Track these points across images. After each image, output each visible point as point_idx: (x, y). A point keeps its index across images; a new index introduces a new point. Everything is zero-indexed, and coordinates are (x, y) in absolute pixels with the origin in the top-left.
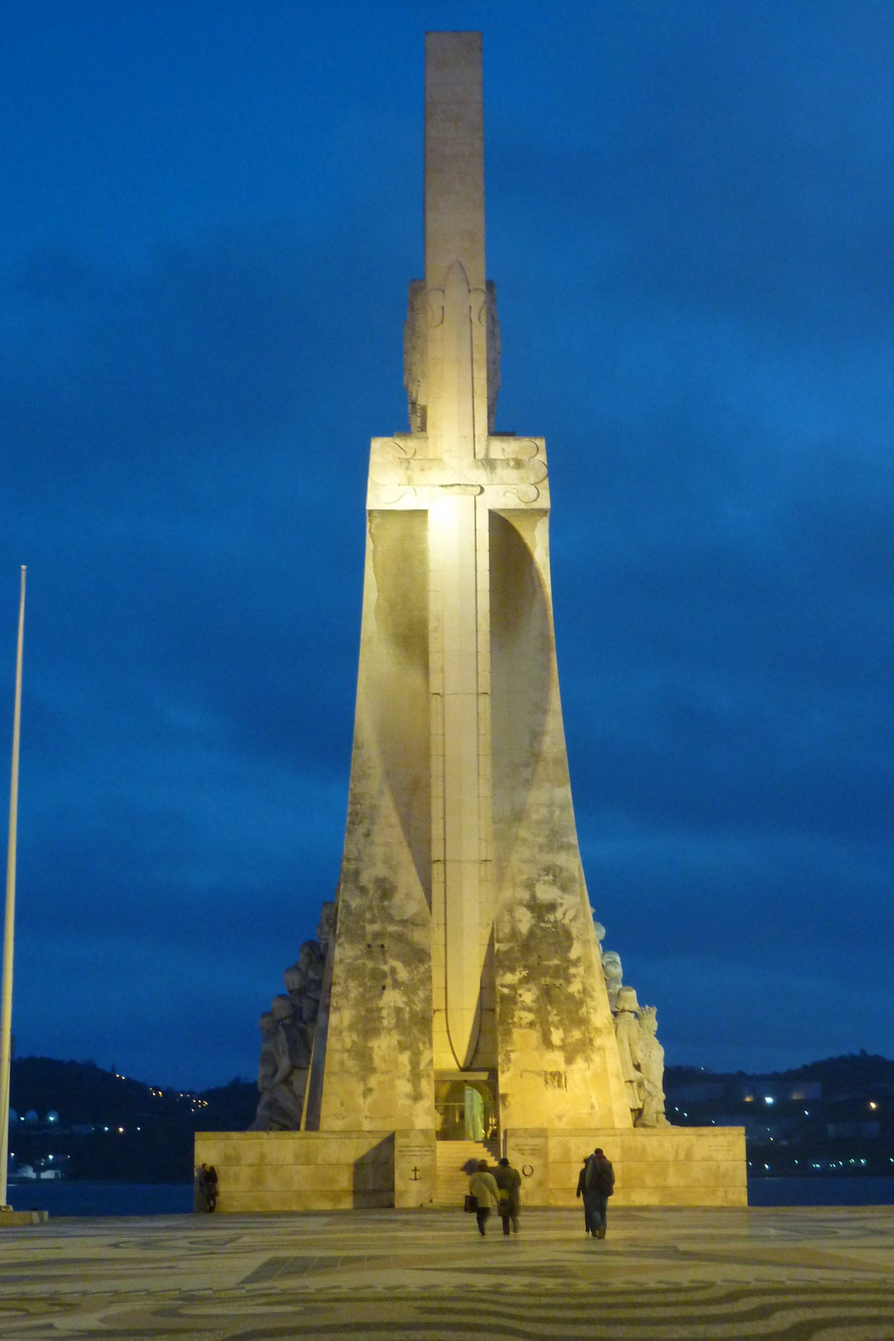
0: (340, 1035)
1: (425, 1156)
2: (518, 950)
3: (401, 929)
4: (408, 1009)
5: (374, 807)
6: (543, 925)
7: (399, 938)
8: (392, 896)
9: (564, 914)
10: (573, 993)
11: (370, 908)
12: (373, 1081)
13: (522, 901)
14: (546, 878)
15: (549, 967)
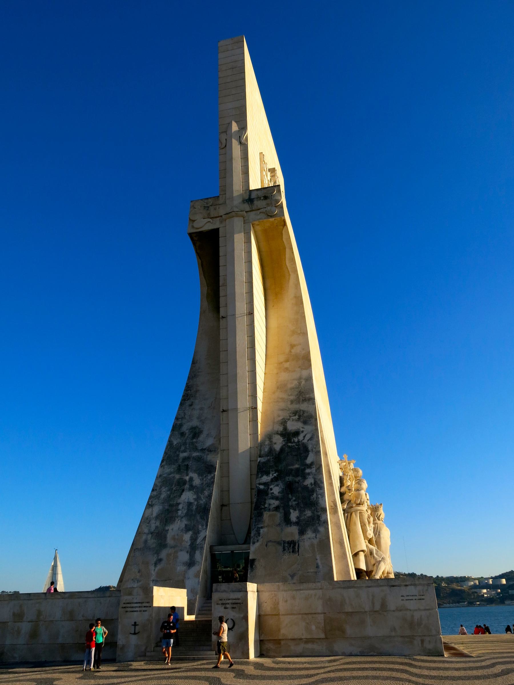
0: (148, 523)
1: (144, 611)
2: (273, 461)
3: (200, 454)
4: (196, 503)
5: (197, 391)
6: (290, 444)
7: (199, 459)
8: (199, 436)
9: (304, 437)
10: (307, 485)
11: (185, 444)
12: (163, 554)
13: (278, 431)
14: (294, 418)
15: (292, 470)
